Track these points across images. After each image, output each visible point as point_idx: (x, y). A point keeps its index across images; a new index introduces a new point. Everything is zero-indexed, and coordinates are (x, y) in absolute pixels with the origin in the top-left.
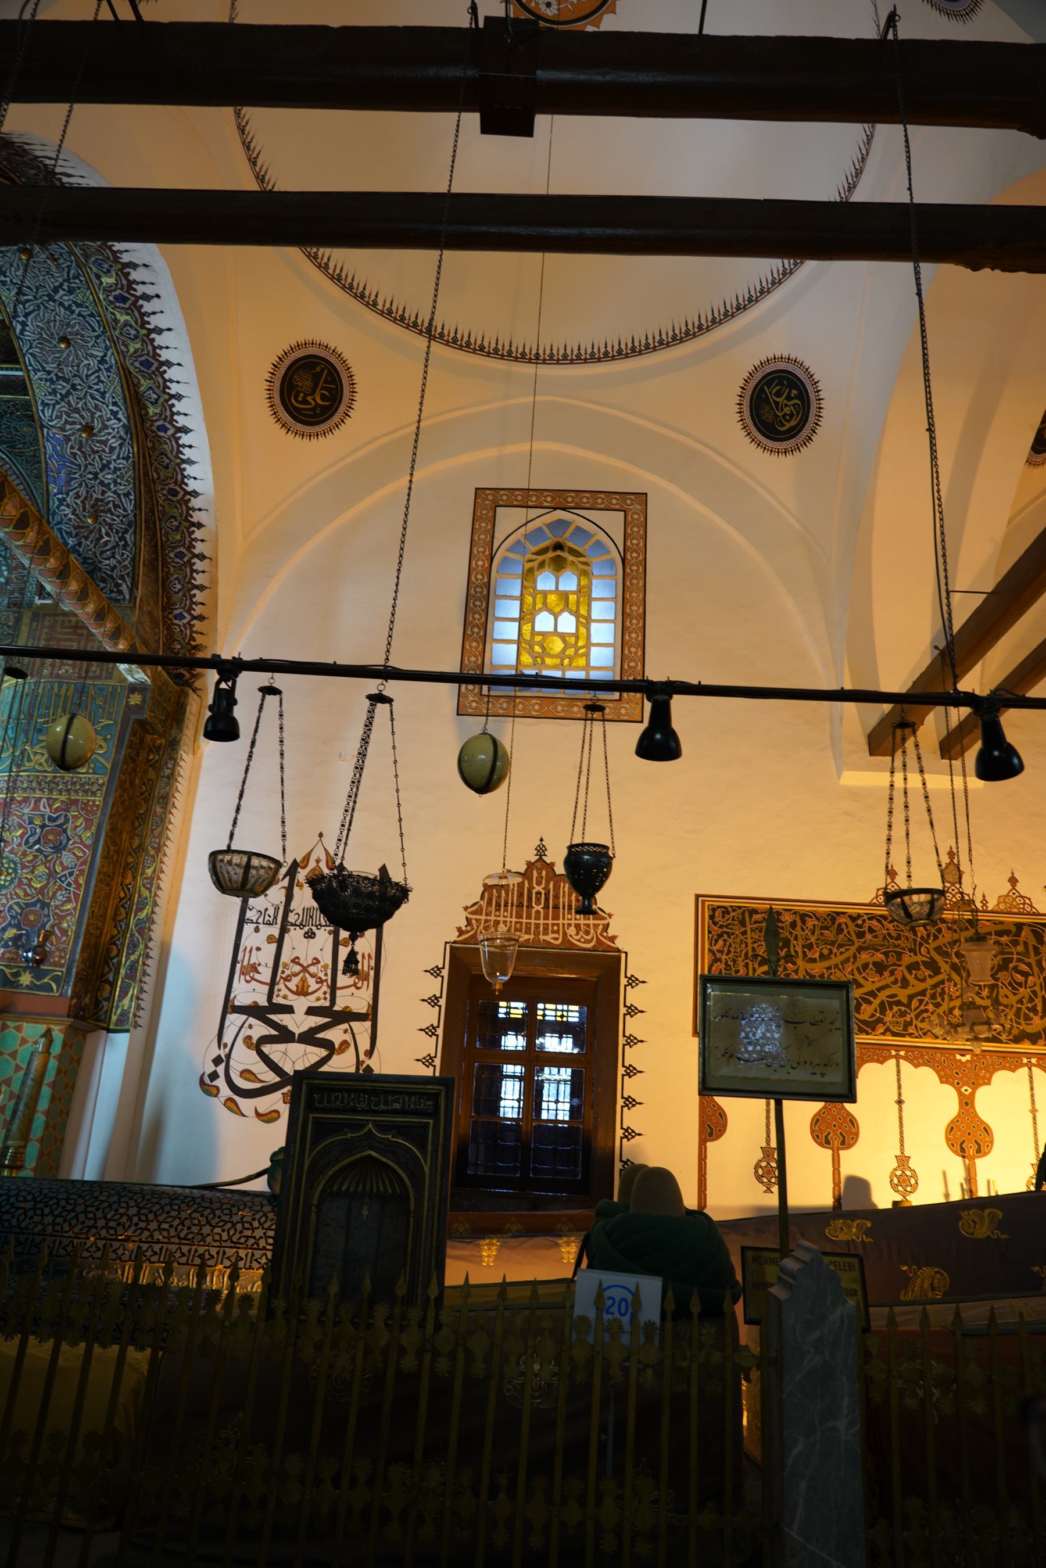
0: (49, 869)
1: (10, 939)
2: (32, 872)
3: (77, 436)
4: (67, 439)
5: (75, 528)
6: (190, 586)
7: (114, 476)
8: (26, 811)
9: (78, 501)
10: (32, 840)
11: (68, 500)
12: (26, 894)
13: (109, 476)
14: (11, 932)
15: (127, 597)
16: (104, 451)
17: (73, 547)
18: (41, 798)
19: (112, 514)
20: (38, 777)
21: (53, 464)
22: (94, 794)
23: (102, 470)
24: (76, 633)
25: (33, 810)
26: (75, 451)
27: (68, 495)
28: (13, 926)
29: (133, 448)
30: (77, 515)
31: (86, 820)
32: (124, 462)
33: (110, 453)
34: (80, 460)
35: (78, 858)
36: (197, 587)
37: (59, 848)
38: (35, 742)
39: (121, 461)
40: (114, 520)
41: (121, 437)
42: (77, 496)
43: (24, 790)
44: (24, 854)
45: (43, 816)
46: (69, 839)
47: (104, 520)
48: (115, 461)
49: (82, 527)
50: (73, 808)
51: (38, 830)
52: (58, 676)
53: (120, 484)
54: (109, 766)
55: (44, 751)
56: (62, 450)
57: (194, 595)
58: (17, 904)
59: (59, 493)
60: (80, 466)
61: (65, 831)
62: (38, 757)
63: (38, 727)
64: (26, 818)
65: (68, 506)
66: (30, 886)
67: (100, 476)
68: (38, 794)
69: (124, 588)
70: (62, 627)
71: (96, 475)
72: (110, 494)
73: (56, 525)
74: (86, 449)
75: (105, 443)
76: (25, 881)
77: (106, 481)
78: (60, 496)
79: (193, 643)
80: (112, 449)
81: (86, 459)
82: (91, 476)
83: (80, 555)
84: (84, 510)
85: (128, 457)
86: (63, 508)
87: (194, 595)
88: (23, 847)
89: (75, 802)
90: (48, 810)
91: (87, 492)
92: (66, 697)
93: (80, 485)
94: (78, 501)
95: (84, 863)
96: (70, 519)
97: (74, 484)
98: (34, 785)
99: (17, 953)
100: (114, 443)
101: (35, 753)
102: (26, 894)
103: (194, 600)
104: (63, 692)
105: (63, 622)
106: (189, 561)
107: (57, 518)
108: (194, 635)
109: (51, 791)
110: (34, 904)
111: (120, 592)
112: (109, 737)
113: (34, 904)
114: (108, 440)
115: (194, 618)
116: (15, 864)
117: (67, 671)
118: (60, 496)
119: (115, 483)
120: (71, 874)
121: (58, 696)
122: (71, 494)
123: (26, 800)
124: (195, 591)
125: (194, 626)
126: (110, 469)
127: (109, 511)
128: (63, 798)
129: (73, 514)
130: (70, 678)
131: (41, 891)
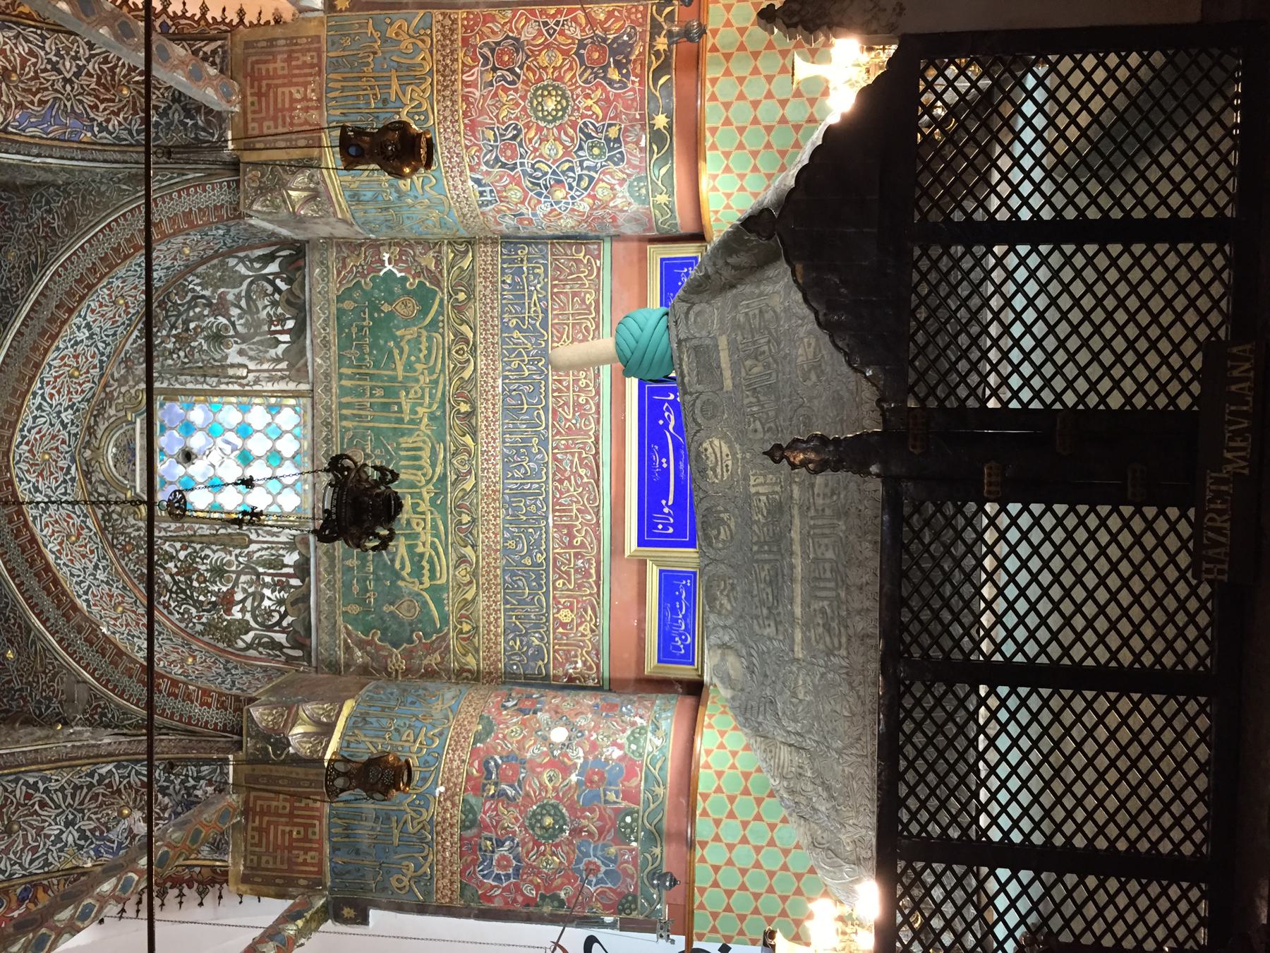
0: (540, 51)
1: (620, 73)
2: (545, 68)
3: (16, 92)
4: (20, 105)
5: (136, 113)
6: (202, 23)
7: (67, 58)
8: (478, 94)
9: (101, 107)
10: (510, 77)
11: (100, 120)
12: (571, 68)
13: (68, 64)
14: (614, 75)
15: (219, 43)
16: (35, 64)
17: (161, 116)
18: (463, 81)
19: (116, 66)
20: (438, 91)
21: (55, 131)
22: (454, 22)
23: (60, 73)
24: (266, 95)
25: (476, 87)
26: (36, 100)
27: (93, 120)
28: (605, 72)
29: (30, 26)
30: (120, 110)
31: (485, 22)
32: (48, 42)
33: (36, 57)
34: (49, 96)
35: (527, 20)
36: (203, 15)
37: (518, 45)
38: (398, 104)
39: (47, 46)
40: (123, 65)
41: (16, 37)
42: (95, 107)
43: (454, 102)
44: (525, 83)
45: (482, 73)
46: (508, 37)
47: (125, 76)
48: (47, 53)
49: (135, 104)
50: (471, 41)
51: (499, 73)
52: (319, 100)
53: (77, 52)
54: (421, 12)
55: (409, 89)
56: (36, 116)
57: (213, 18)
58: (581, 75)
59: (92, 131)
60: (55, 99)
61: (498, 44)
62: (415, 95)
63: (380, 105)
64: (485, 92)
65: (108, 121)
66: (561, 66)
67: (68, 76)
68: (459, 85)
69: (208, 49)
70: (260, 111)
71: (66, 81)
72: (90, 67)
73: (132, 136)
74: (34, 85)
75: (24, 61)
76: (556, 74)
77: (74, 69)
78: (96, 129)
79: (272, 23)
80: (31, 53)
81: (47, 89)
82: (68, 87)
83: (170, 107)
84: (113, 101)
85: (41, 35)
86: (110, 127)
87: (213, 18)
88: (519, 85)
89: (465, 41)
90: (475, 70)
91: (89, 94)
92: (345, 79)
93: (81, 102)
94: (101, 107)
95: (533, 13)
96: (125, 119)
97: (79, 109)
98: (448, 93)
99: (635, 61)
100: (23, 48)
101: (412, 99)
102: (571, 68)
103: (219, 20)
104: (338, 85)
105: (254, 112)
106: (172, 19)
107: (124, 134)
108: (262, 22)
109: (454, 72)
110: (580, 56)
111: (214, 52)
112: (388, 21)
113: (580, 56)
114: (20, 54)
115: (241, 21)
116: (537, 89)
117: (313, 91)
118: (96, 129)
119: (76, 58)
120: (545, 24)
121: (343, 89)
122: (92, 115)
123: (465, 98)
124: (209, 17)
125: (251, 23)
126: (58, 62)
127: (112, 69)
128: (461, 55)
129: (117, 114)
130: (320, 85)
131: (565, 53)
